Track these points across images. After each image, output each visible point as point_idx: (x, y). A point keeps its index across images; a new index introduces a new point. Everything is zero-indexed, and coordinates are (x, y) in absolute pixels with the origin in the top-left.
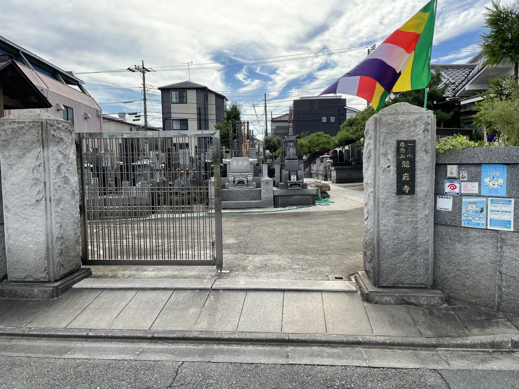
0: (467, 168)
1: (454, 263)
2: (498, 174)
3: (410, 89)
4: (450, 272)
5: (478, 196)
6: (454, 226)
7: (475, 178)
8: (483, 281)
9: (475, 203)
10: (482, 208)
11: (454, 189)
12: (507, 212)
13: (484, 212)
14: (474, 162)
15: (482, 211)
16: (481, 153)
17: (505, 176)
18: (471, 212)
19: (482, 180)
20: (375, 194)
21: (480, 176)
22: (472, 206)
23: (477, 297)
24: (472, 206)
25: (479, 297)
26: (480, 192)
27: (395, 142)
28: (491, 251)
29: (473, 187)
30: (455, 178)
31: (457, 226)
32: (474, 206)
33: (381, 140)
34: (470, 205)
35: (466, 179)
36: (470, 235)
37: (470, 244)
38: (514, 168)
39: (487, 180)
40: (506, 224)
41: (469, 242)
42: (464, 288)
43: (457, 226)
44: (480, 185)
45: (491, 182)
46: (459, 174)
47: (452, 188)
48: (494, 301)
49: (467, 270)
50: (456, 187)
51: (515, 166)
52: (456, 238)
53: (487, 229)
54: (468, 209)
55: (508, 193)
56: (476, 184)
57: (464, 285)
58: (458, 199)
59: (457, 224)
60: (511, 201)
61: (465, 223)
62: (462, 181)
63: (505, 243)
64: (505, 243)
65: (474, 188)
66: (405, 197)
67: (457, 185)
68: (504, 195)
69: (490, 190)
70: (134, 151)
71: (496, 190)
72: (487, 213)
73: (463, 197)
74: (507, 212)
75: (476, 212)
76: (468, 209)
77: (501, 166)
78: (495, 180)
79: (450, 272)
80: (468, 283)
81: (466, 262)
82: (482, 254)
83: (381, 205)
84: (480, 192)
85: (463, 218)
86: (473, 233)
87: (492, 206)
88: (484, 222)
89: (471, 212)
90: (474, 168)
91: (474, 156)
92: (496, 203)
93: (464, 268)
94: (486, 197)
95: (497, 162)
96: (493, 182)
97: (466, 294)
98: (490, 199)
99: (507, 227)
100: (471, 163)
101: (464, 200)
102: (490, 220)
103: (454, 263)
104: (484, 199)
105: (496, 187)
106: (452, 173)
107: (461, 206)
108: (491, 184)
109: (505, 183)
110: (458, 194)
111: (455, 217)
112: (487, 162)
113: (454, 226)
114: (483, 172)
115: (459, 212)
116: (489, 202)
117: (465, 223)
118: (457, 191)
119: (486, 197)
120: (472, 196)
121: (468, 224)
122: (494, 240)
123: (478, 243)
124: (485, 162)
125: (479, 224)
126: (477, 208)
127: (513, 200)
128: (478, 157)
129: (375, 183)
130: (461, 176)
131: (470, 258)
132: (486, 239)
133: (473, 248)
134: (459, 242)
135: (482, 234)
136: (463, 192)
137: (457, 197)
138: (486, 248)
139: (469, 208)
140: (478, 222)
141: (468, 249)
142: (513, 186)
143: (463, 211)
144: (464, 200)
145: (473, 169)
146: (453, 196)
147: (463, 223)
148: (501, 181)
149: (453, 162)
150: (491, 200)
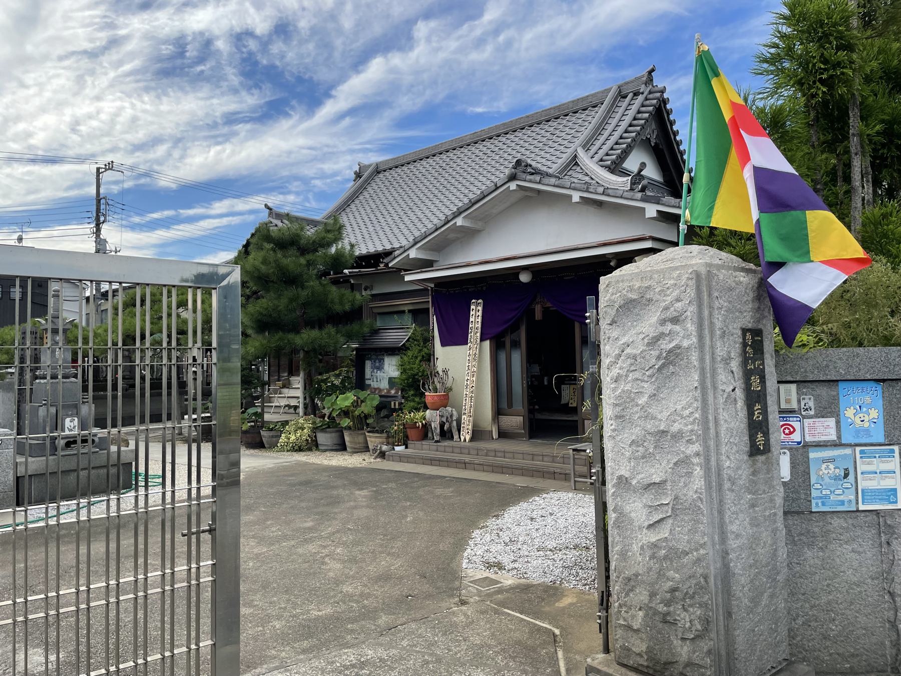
0: (813, 389)
1: (803, 594)
2: (868, 399)
3: (807, 212)
4: (798, 615)
5: (835, 445)
6: (798, 513)
7: (829, 409)
8: (862, 619)
9: (832, 460)
10: (846, 470)
11: (791, 433)
12: (889, 472)
13: (851, 477)
14: (829, 378)
15: (846, 476)
16: (840, 359)
17: (880, 402)
18: (827, 480)
19: (841, 413)
20: (707, 460)
21: (838, 405)
22: (827, 468)
23: (853, 655)
24: (827, 468)
25: (857, 655)
26: (839, 437)
27: (740, 333)
28: (869, 554)
29: (826, 429)
30: (792, 411)
31: (803, 513)
32: (832, 466)
33: (718, 324)
34: (824, 466)
35: (812, 413)
36: (830, 527)
37: (832, 547)
38: (893, 387)
39: (850, 413)
40: (889, 496)
41: (831, 543)
42: (828, 643)
43: (803, 513)
44: (838, 423)
45: (857, 417)
46: (799, 402)
47: (787, 431)
48: (884, 655)
49: (829, 603)
50: (794, 430)
51: (894, 383)
52: (802, 537)
53: (858, 511)
54: (821, 473)
55: (887, 436)
56: (831, 422)
57: (826, 637)
58: (801, 453)
59: (803, 508)
60: (893, 451)
61: (817, 504)
62: (804, 417)
63: (894, 533)
64: (894, 533)
65: (828, 430)
66: (761, 458)
67: (797, 425)
68: (882, 440)
69: (858, 432)
70: (402, 308)
71: (867, 431)
72: (856, 478)
73: (810, 449)
74: (889, 472)
75: (836, 478)
76: (821, 473)
77: (873, 384)
78: (864, 411)
79: (798, 615)
80: (834, 629)
81: (828, 585)
82: (855, 564)
83: (727, 485)
84: (839, 437)
85: (814, 494)
86: (836, 522)
87: (863, 463)
88: (853, 497)
89: (827, 480)
90: (825, 389)
91: (827, 366)
92: (869, 457)
93: (824, 599)
94: (850, 445)
95: (869, 378)
96: (861, 415)
97: (831, 655)
98: (858, 449)
99: (891, 503)
100: (824, 378)
101: (813, 455)
102: (863, 491)
103: (803, 594)
104: (848, 451)
105: (866, 425)
106: (788, 401)
107: (808, 467)
108: (858, 421)
109: (881, 417)
110: (799, 443)
111: (798, 492)
112: (853, 378)
113: (798, 513)
114: (841, 397)
115: (804, 482)
116: (858, 456)
117: (817, 504)
118: (796, 437)
119: (850, 445)
120: (826, 446)
121: (823, 504)
122: (873, 532)
123: (846, 543)
124: (849, 377)
125: (842, 503)
126: (837, 470)
127: (896, 448)
128: (835, 368)
129: (706, 429)
130: (803, 406)
131: (836, 575)
132: (859, 532)
133: (838, 553)
134: (811, 545)
135: (850, 521)
136: (808, 439)
137: (797, 449)
138: (861, 550)
139: (823, 469)
140: (841, 498)
141: (829, 557)
142: (894, 422)
143: (813, 480)
144: (813, 455)
145: (823, 391)
146: (790, 449)
147: (814, 502)
148: (874, 414)
149: (789, 378)
150: (862, 452)
